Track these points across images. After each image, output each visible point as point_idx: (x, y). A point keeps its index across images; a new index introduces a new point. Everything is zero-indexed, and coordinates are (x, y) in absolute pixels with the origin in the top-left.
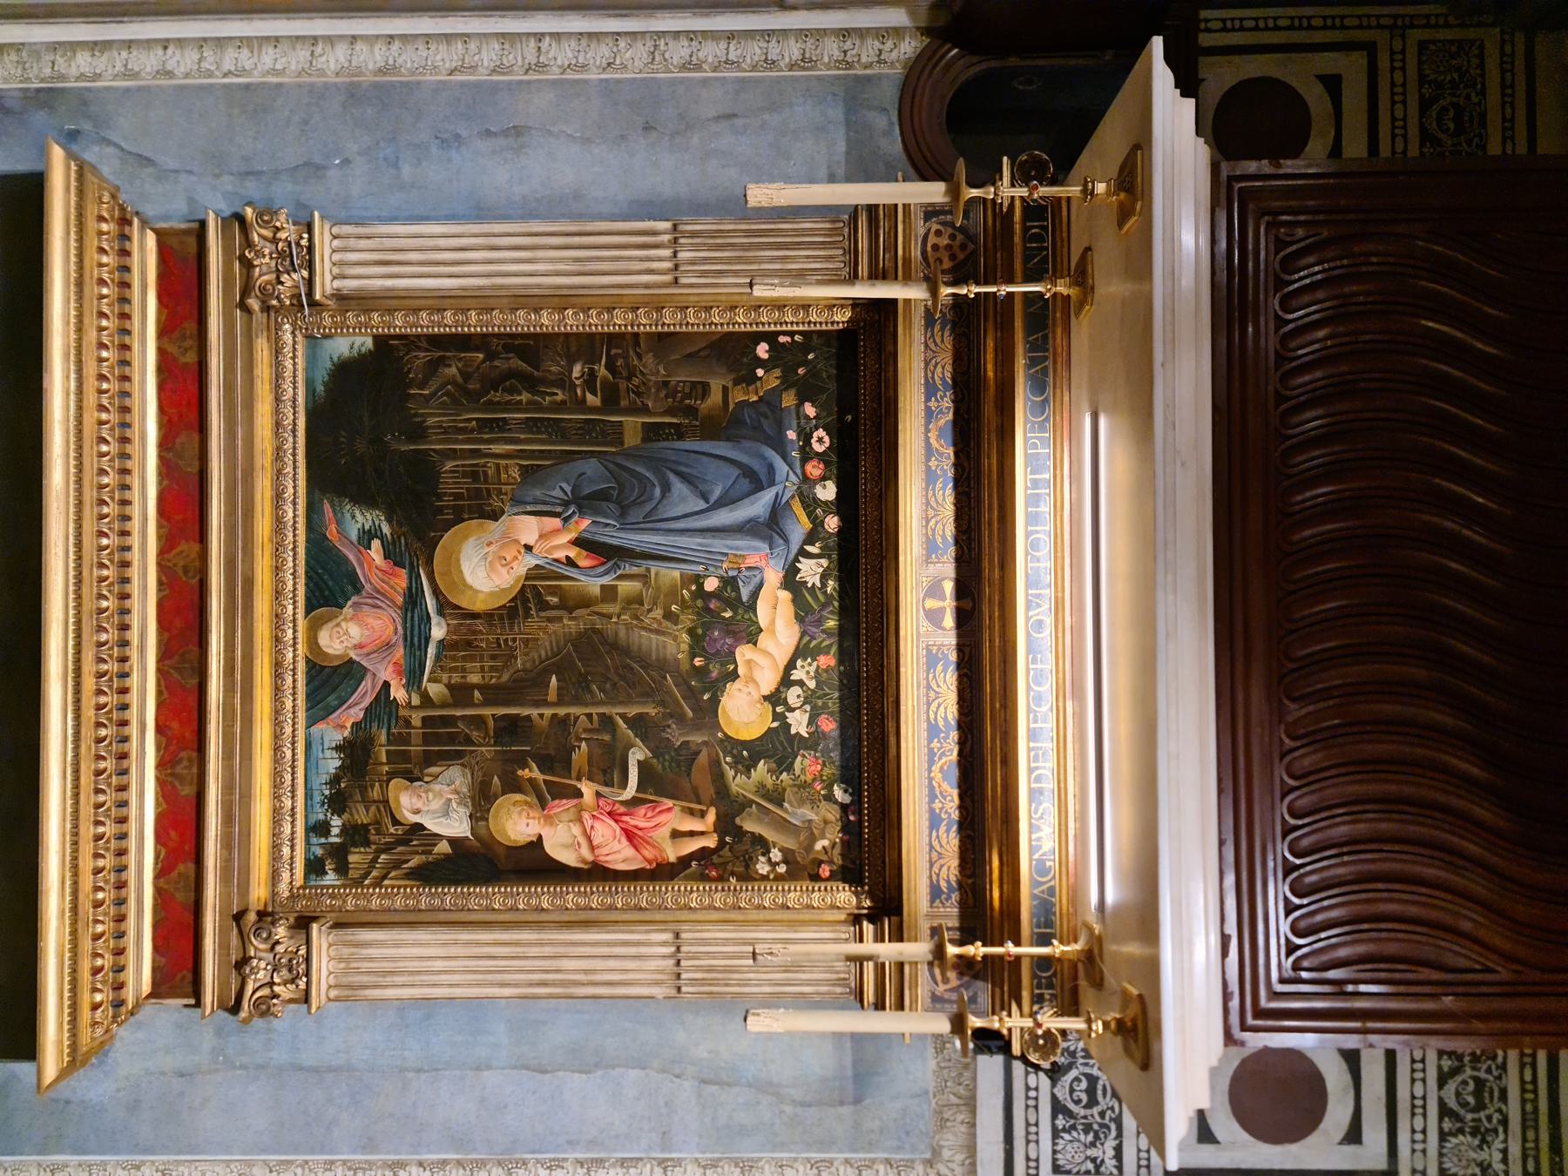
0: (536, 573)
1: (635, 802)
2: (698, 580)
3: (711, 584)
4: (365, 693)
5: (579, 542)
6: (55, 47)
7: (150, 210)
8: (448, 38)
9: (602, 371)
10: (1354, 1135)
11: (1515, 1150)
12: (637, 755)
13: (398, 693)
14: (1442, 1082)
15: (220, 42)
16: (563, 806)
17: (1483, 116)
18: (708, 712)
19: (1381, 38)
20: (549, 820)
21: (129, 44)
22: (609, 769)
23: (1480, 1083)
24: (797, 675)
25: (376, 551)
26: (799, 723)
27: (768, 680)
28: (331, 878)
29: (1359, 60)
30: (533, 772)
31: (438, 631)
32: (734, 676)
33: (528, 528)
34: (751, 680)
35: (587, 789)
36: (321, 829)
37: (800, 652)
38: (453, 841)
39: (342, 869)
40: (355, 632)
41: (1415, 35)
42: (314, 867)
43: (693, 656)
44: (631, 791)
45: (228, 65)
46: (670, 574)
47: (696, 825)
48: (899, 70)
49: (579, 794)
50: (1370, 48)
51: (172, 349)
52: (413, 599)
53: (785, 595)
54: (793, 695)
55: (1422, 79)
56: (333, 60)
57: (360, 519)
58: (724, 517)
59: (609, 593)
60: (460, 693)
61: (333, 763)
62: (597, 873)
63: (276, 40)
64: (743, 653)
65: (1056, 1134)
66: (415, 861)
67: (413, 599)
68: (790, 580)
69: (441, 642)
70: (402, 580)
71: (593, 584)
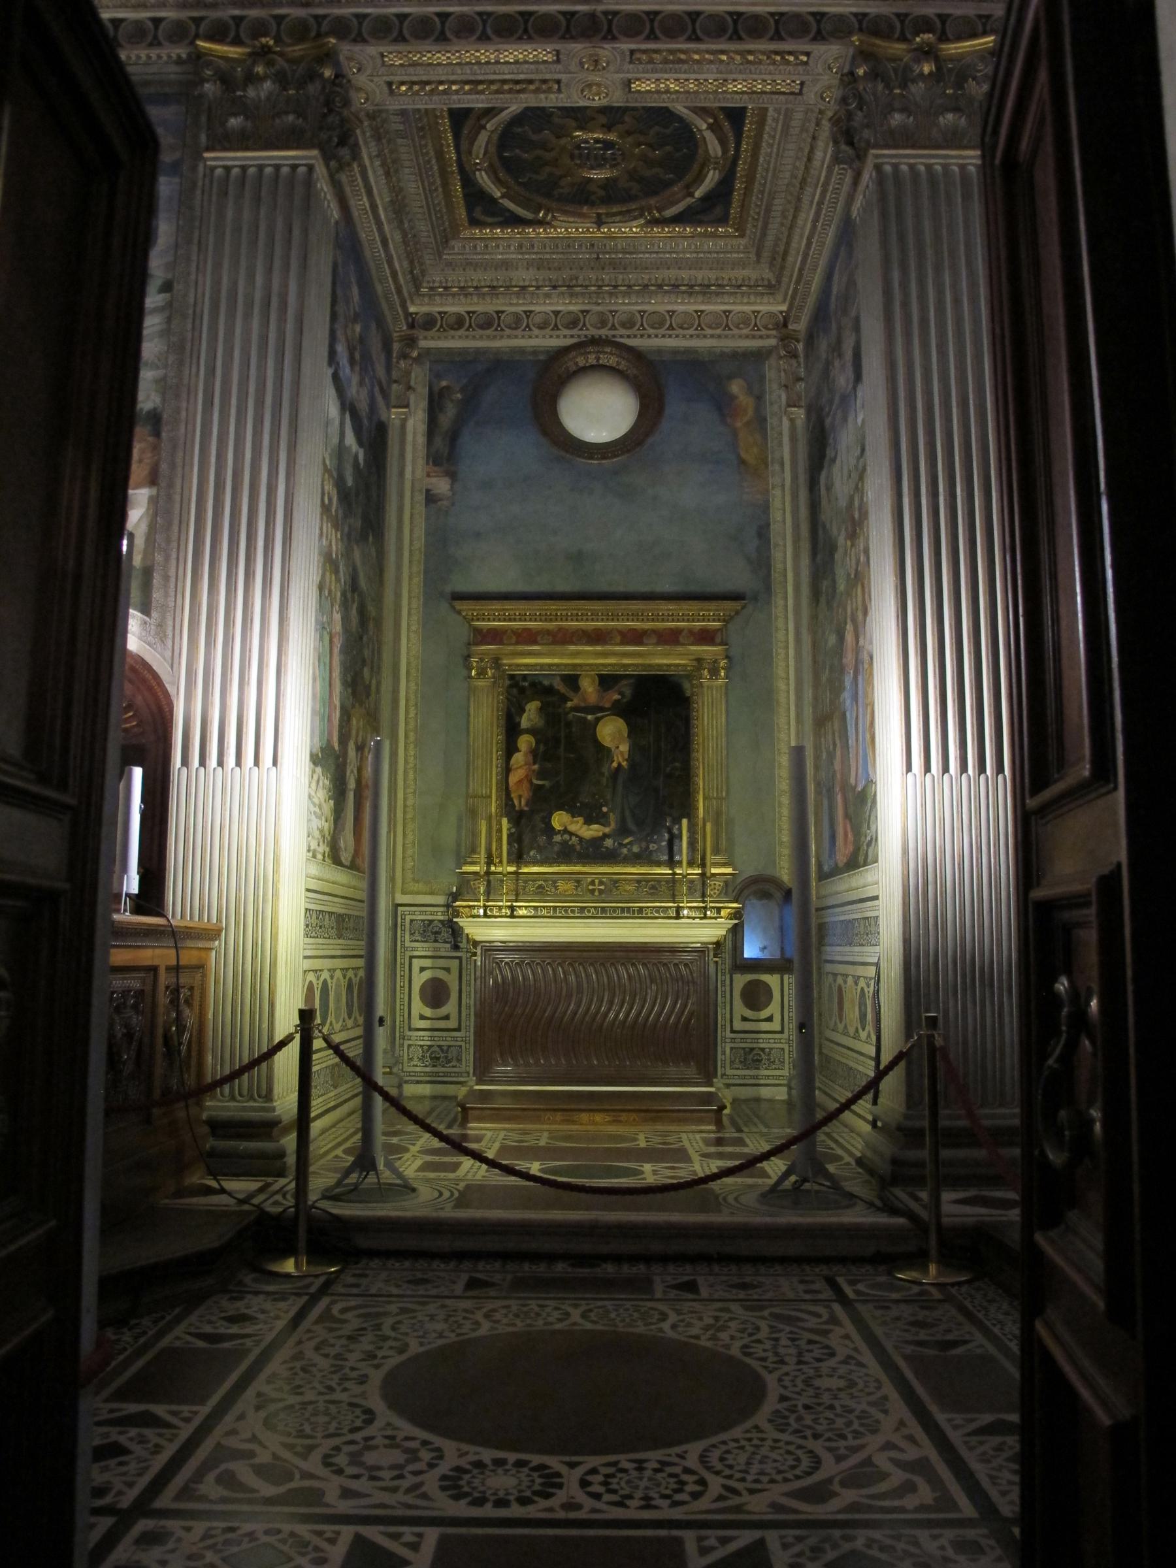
0: (609, 750)
1: (531, 783)
2: (606, 805)
3: (605, 809)
4: (570, 694)
5: (620, 765)
6: (786, 593)
7: (729, 626)
8: (789, 723)
9: (677, 773)
10: (422, 1017)
11: (418, 1069)
12: (546, 783)
13: (569, 704)
14: (439, 1046)
15: (787, 648)
16: (530, 758)
17: (758, 1069)
18: (560, 808)
19: (785, 1035)
20: (526, 755)
21: (786, 618)
22: (541, 774)
23: (438, 1059)
24: (574, 838)
25: (616, 697)
26: (557, 838)
27: (572, 828)
28: (508, 682)
29: (778, 1028)
30: (542, 748)
31: (589, 717)
32: (573, 816)
33: (624, 748)
34: (572, 823)
35: (536, 767)
36: (525, 677)
37: (581, 839)
38: (519, 723)
39: (511, 686)
40: (590, 690)
41: (786, 1047)
42: (512, 677)
43: (581, 803)
44: (535, 782)
45: (780, 651)
46: (609, 797)
47: (523, 802)
48: (778, 875)
49: (534, 763)
50: (782, 1032)
51: (684, 634)
52: (602, 709)
53: (601, 834)
54: (566, 837)
55: (771, 1049)
56: (781, 685)
57: (628, 692)
58: (627, 813)
59: (602, 774)
60: (569, 724)
61: (546, 682)
62: (507, 770)
63: (788, 666)
64: (581, 820)
65: (423, 921)
66: (513, 710)
67: (602, 709)
68: (605, 836)
69: (585, 719)
70: (607, 705)
71: (605, 770)
